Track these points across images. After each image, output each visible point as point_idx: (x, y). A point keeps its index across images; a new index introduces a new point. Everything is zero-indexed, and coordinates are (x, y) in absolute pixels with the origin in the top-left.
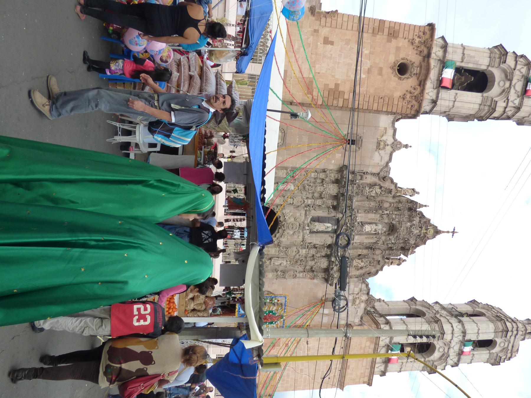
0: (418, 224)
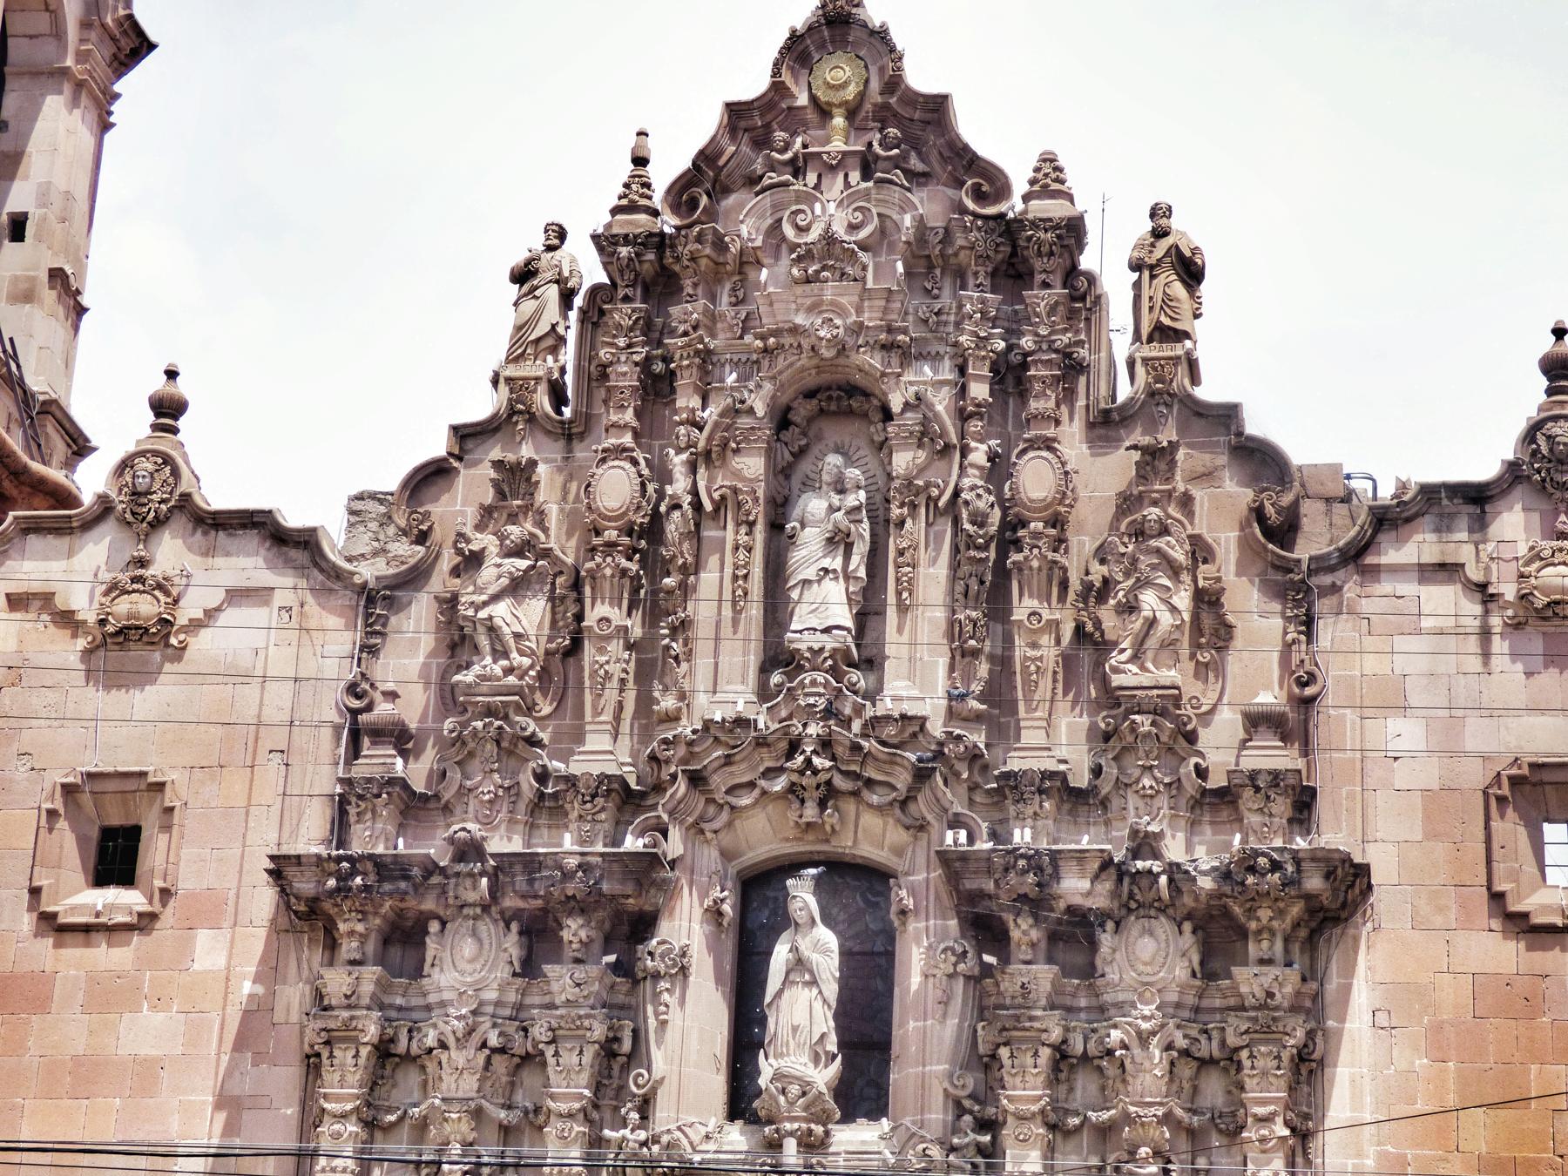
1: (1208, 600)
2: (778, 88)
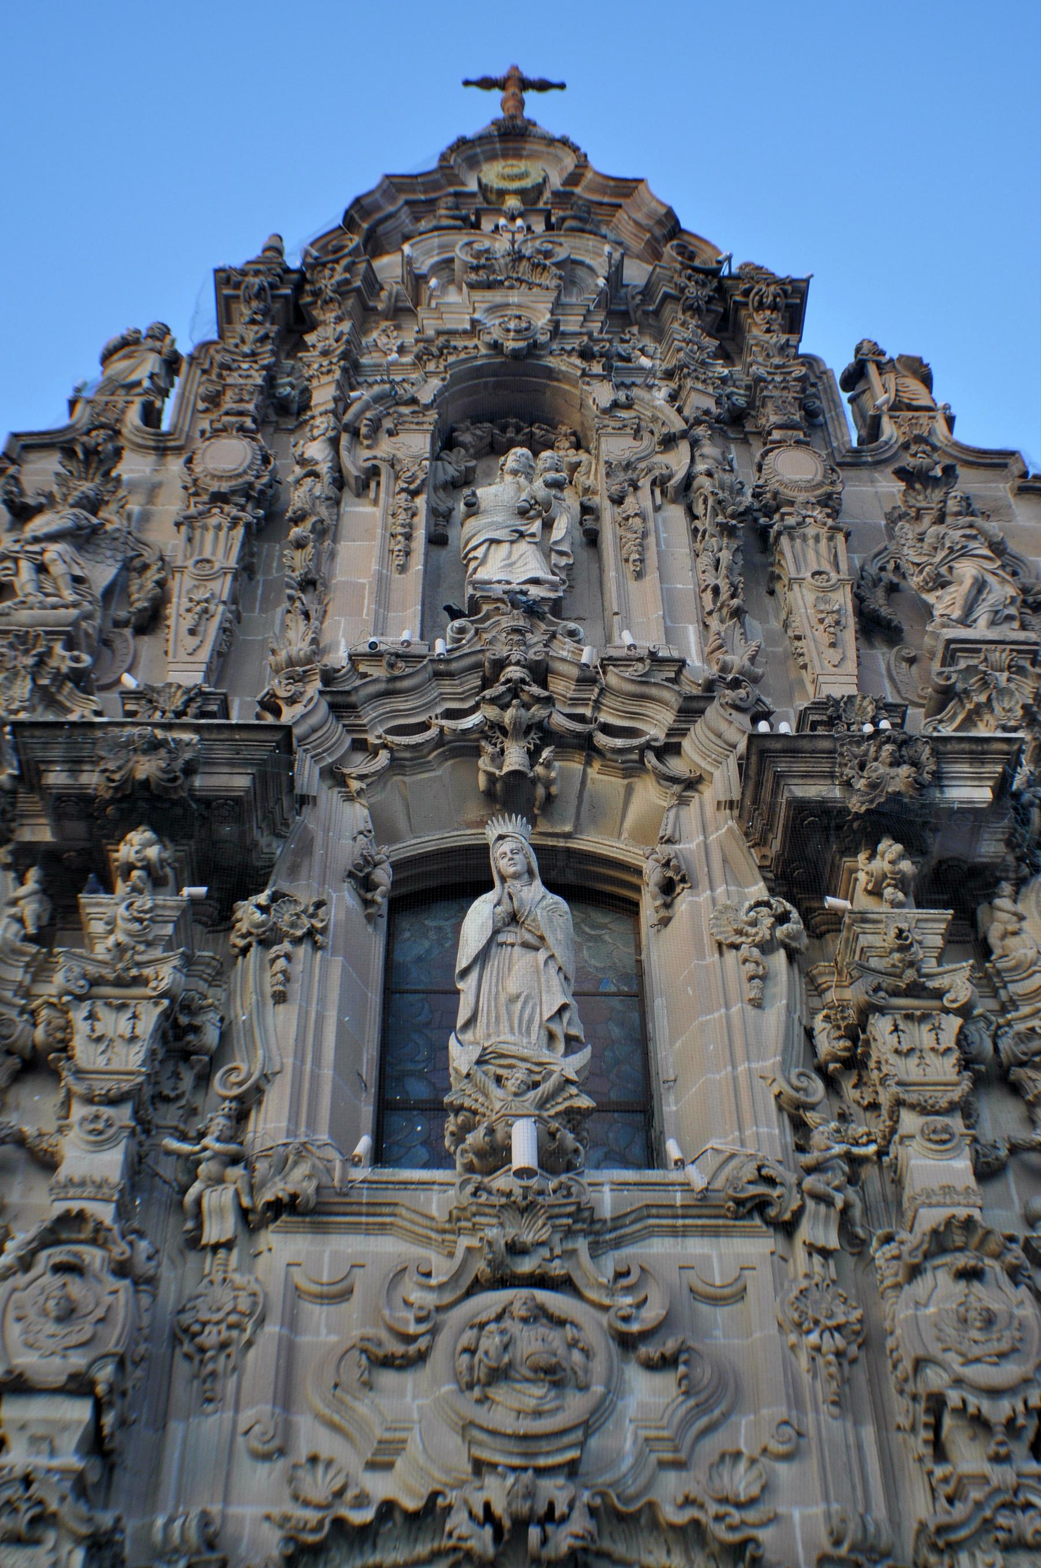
0: (435, 240)
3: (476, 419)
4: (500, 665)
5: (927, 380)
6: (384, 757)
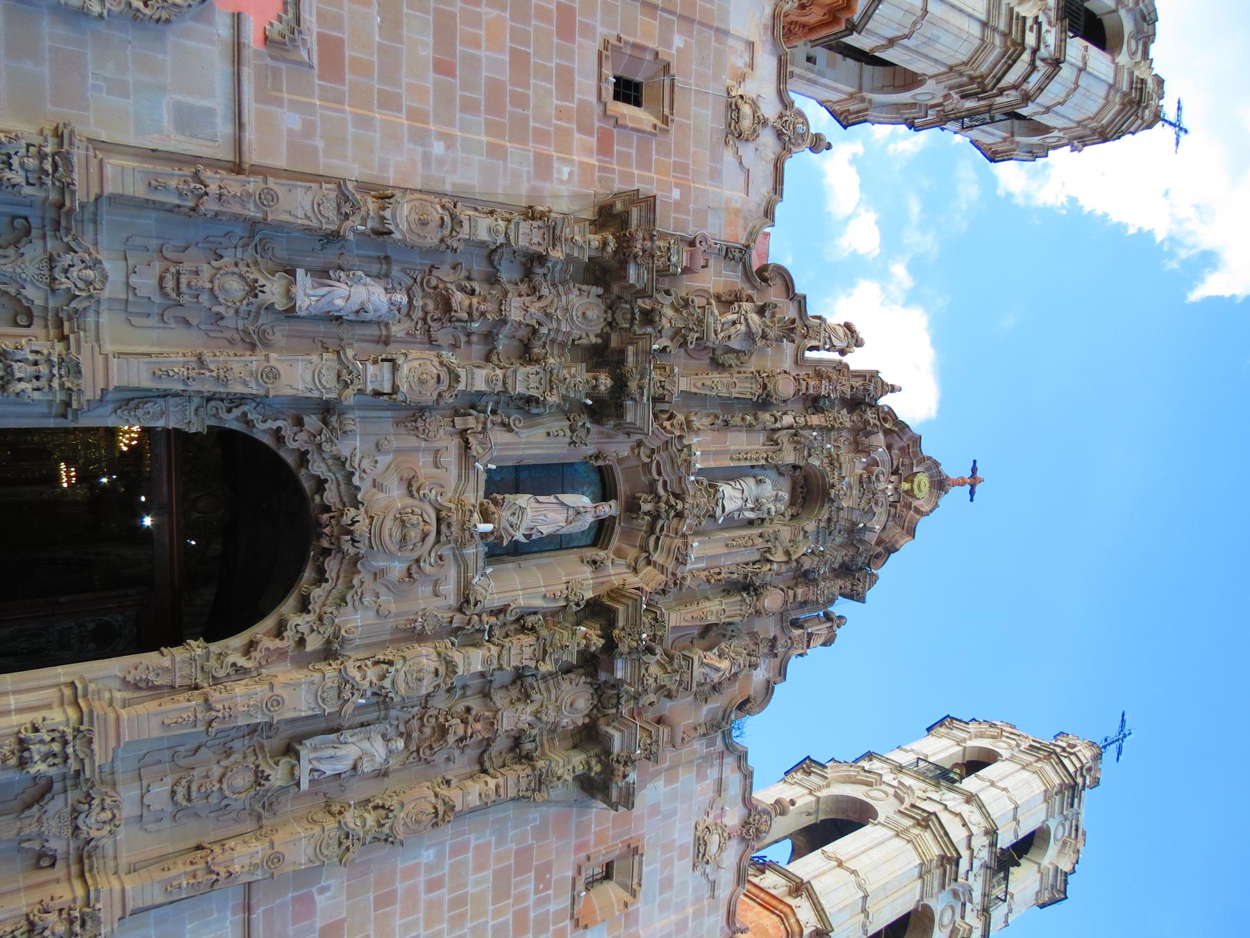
0: (887, 458)
1: (716, 688)
2: (924, 459)
3: (806, 478)
4: (683, 500)
5: (824, 644)
6: (648, 460)
